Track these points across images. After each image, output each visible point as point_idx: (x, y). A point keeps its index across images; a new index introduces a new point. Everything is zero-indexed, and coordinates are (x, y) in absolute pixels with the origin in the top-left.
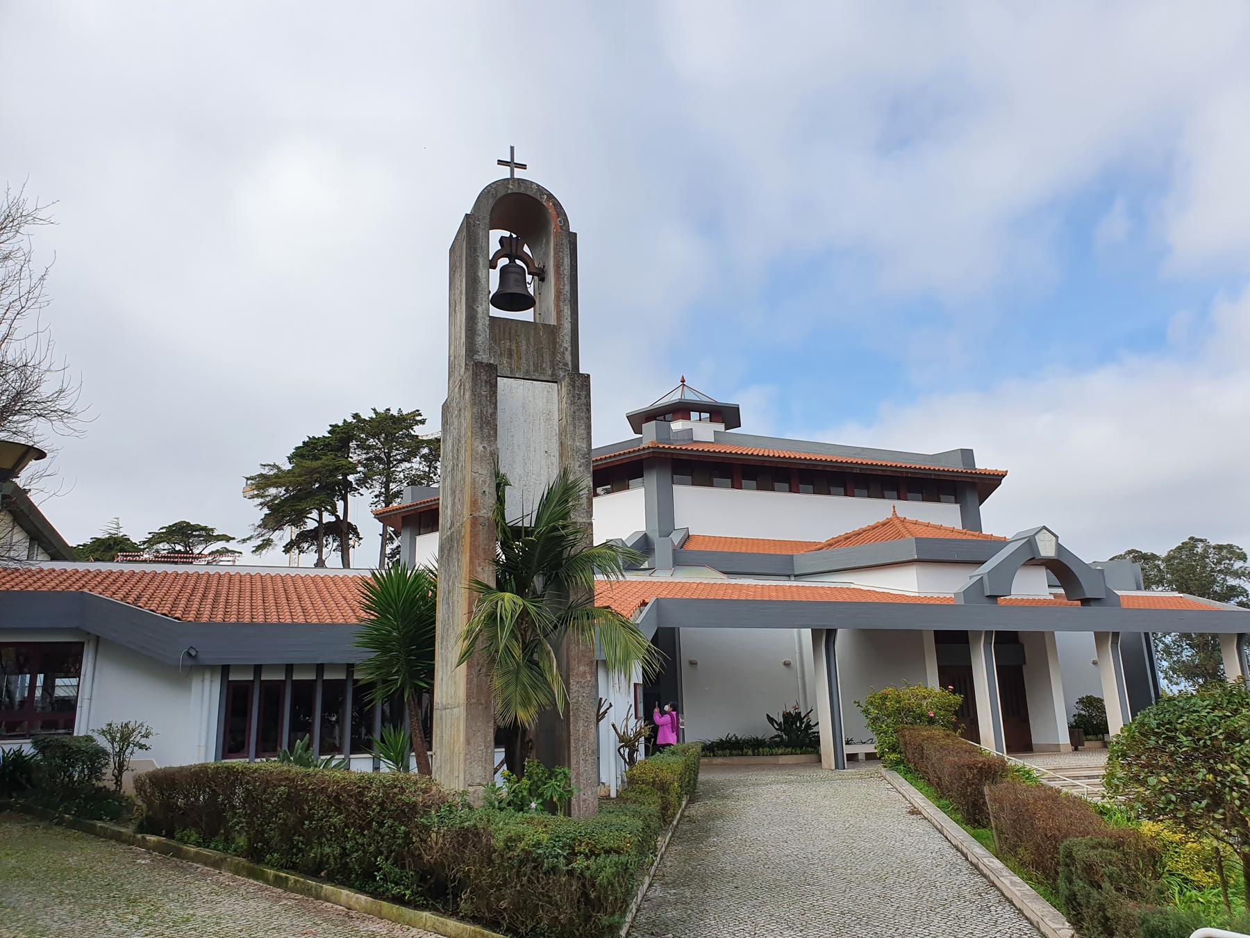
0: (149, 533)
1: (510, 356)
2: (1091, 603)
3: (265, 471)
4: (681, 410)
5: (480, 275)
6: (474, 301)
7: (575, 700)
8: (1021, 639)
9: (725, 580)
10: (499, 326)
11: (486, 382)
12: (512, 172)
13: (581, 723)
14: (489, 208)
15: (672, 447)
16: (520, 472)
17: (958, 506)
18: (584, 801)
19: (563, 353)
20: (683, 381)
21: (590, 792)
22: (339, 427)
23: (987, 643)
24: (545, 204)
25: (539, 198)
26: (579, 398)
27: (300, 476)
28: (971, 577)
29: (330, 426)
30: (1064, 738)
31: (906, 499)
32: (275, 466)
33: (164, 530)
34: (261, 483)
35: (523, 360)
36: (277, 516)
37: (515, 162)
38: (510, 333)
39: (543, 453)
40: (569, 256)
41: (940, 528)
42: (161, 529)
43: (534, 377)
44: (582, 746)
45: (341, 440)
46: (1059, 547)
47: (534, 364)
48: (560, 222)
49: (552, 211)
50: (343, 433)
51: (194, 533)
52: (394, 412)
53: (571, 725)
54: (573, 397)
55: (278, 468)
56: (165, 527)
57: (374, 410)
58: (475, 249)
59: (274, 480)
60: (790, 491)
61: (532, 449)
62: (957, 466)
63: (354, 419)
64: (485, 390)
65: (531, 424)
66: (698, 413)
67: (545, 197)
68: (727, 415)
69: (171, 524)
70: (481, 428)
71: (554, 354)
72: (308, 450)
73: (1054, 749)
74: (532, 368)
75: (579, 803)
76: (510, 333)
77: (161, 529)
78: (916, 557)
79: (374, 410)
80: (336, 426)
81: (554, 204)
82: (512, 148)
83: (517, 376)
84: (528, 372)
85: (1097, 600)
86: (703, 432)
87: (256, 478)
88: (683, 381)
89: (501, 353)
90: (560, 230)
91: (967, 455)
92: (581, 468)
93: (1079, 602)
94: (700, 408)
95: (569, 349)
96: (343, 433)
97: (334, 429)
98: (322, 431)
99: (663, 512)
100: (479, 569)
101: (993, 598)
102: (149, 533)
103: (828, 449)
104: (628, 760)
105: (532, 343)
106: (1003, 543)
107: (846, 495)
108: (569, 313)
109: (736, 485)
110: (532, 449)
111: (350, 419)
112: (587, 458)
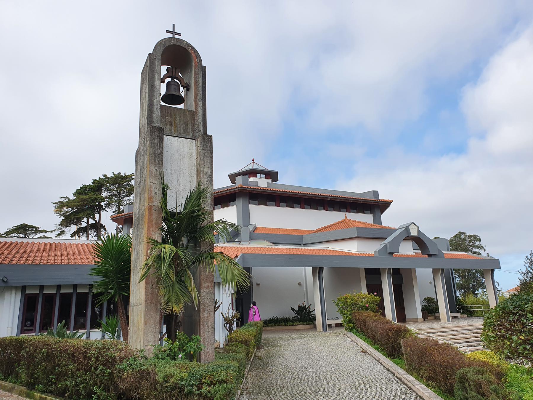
0: (8, 229)
1: (171, 124)
2: (432, 256)
3: (62, 200)
4: (252, 173)
5: (156, 83)
6: (152, 96)
7: (203, 301)
8: (401, 271)
9: (273, 246)
10: (165, 110)
11: (158, 136)
12: (174, 36)
13: (206, 312)
14: (161, 51)
15: (249, 187)
16: (175, 184)
17: (372, 215)
18: (208, 352)
19: (198, 125)
20: (253, 160)
21: (210, 348)
22: (96, 180)
23: (389, 274)
24: (190, 51)
25: (187, 48)
26: (207, 147)
27: (78, 202)
28: (381, 245)
29: (93, 180)
30: (420, 315)
32: (67, 198)
33: (15, 228)
34: (60, 206)
35: (178, 127)
36: (67, 221)
37: (175, 32)
38: (171, 113)
39: (188, 175)
40: (202, 77)
41: (366, 224)
42: (13, 227)
43: (183, 136)
44: (207, 324)
45: (98, 186)
46: (419, 232)
47: (183, 129)
48: (198, 60)
49: (193, 55)
50: (99, 183)
51: (29, 229)
52: (122, 174)
53: (201, 313)
54: (204, 146)
55: (68, 199)
56: (15, 226)
57: (113, 173)
58: (153, 71)
59: (66, 204)
60: (301, 208)
61: (182, 173)
62: (371, 198)
63: (104, 177)
64: (157, 140)
65: (181, 160)
66: (260, 175)
67: (190, 48)
68: (272, 176)
69: (18, 225)
70: (155, 160)
71: (193, 125)
72: (83, 191)
73: (416, 321)
74: (182, 132)
75: (205, 353)
76: (171, 113)
77: (13, 227)
78: (357, 236)
79: (113, 173)
80: (96, 180)
81: (195, 52)
82: (174, 25)
83: (174, 135)
84: (180, 133)
85: (435, 255)
86: (262, 183)
87: (58, 203)
88: (253, 160)
89: (166, 123)
90: (197, 65)
91: (376, 193)
92: (208, 183)
93: (427, 256)
94: (261, 172)
95: (202, 123)
96: (99, 183)
97: (95, 181)
98: (89, 182)
99: (245, 216)
100: (153, 233)
101: (391, 254)
102: (8, 229)
103: (316, 190)
104: (228, 330)
105: (182, 119)
106: (394, 230)
107: (324, 210)
108: (202, 105)
109: (277, 205)
110: (182, 173)
111: (102, 177)
112: (210, 177)
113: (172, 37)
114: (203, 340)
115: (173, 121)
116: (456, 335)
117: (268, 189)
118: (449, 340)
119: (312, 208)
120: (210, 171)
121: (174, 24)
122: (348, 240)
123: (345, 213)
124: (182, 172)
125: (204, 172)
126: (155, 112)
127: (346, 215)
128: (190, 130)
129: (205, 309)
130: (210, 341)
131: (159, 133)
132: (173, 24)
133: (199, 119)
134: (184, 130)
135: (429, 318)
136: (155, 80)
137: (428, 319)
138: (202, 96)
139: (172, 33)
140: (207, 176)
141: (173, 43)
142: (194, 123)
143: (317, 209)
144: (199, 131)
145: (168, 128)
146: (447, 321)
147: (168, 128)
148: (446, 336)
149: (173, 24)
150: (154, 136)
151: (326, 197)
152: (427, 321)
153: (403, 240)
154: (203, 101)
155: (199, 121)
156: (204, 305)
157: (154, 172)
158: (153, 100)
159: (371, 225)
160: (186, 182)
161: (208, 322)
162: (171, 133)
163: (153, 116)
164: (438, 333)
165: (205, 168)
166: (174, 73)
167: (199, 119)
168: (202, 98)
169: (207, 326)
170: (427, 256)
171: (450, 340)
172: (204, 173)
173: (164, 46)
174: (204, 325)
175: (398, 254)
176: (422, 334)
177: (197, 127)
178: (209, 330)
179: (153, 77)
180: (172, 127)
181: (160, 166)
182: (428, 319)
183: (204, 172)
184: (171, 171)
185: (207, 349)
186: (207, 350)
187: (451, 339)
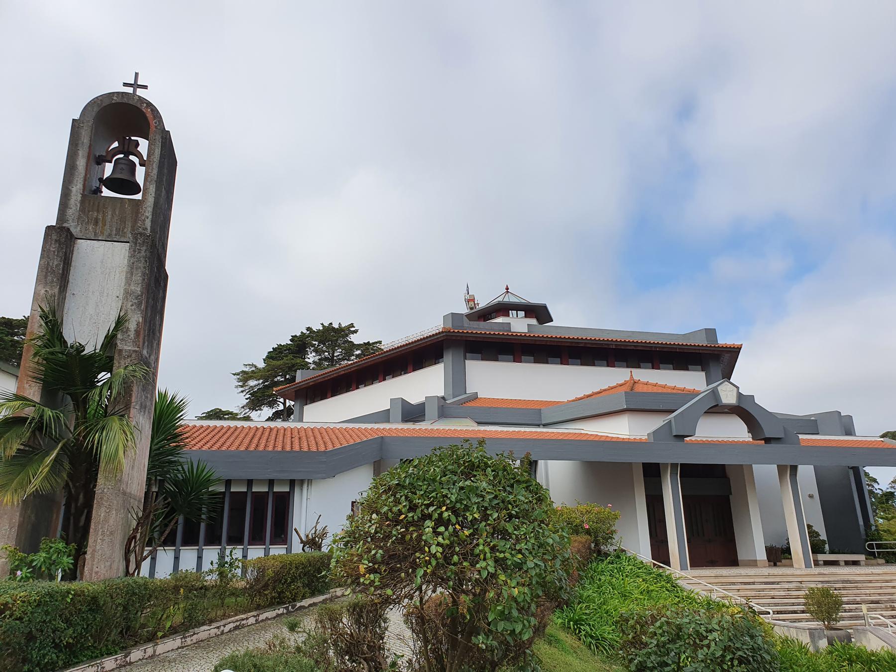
0: (196, 417)
1: (96, 222)
2: (772, 442)
3: (247, 369)
4: (502, 309)
5: (78, 163)
6: (70, 183)
7: (100, 491)
8: (729, 473)
9: (477, 428)
10: (90, 201)
11: (56, 241)
12: (135, 91)
13: (103, 509)
14: (94, 114)
15: (465, 331)
16: (91, 313)
17: (703, 374)
18: (97, 573)
19: (144, 220)
20: (507, 289)
21: (103, 566)
22: (297, 336)
23: (673, 474)
24: (144, 110)
25: (139, 106)
26: (139, 252)
27: (268, 371)
28: (664, 421)
29: (292, 336)
30: (761, 555)
31: (659, 369)
32: (253, 365)
33: (205, 415)
34: (244, 377)
35: (107, 226)
36: (257, 401)
37: (139, 84)
38: (98, 206)
39: (115, 298)
40: (160, 148)
41: (664, 387)
42: (203, 414)
43: (115, 239)
44: (102, 528)
45: (298, 346)
46: (740, 396)
47: (116, 229)
48: (156, 123)
49: (149, 115)
50: (299, 341)
51: (225, 417)
52: (336, 326)
53: (94, 511)
54: (134, 251)
55: (256, 367)
56: (205, 413)
57: (322, 324)
58: (77, 145)
59: (251, 374)
60: (561, 364)
61: (105, 294)
62: (702, 341)
63: (308, 331)
64: (54, 247)
65: (107, 275)
66: (516, 312)
67: (145, 105)
68: (539, 313)
69: (209, 411)
70: (46, 277)
71: (135, 221)
72: (277, 353)
73: (753, 564)
74: (114, 232)
75: (91, 574)
76: (98, 206)
77: (203, 414)
78: (625, 407)
79: (322, 324)
80: (296, 336)
81: (152, 110)
82: (137, 74)
83: (100, 239)
84: (110, 235)
85: (777, 440)
86: (519, 324)
87: (239, 374)
88: (507, 289)
89: (88, 221)
90: (155, 129)
91: (711, 333)
92: (133, 307)
93: (764, 441)
94: (517, 307)
95: (150, 217)
96: (299, 341)
97: (294, 339)
98: (286, 341)
99: (457, 380)
100: (27, 386)
101: (681, 437)
102: (196, 417)
103: (608, 334)
104: (134, 540)
105: (117, 213)
106: (698, 393)
107: (608, 366)
108: (154, 190)
109: (517, 360)
110: (105, 294)
111: (305, 331)
112: (139, 299)
113: (132, 92)
114: (91, 552)
115: (100, 217)
116: (794, 590)
117: (494, 333)
118: (770, 597)
119: (583, 364)
120: (139, 289)
121: (137, 72)
122: (618, 415)
123: (629, 370)
124: (105, 293)
125: (130, 291)
126: (72, 206)
127: (631, 372)
128: (128, 230)
129: (102, 504)
130: (104, 556)
131: (59, 235)
132: (136, 73)
133: (147, 212)
134: (118, 230)
135: (783, 561)
136: (78, 158)
137: (781, 562)
138: (157, 177)
139: (132, 87)
140: (134, 298)
141: (115, 100)
142: (137, 217)
143: (547, 363)
144: (144, 230)
145: (90, 228)
146: (804, 566)
147: (90, 228)
148: (768, 590)
149: (136, 73)
150: (50, 240)
151: (606, 343)
152: (779, 566)
153: (705, 413)
154: (156, 184)
155: (147, 214)
156: (100, 498)
157: (41, 294)
158: (70, 188)
159: (674, 389)
160: (111, 309)
161: (105, 524)
162: (95, 235)
163: (68, 211)
164: (754, 584)
165: (132, 285)
166: (126, 147)
167: (147, 212)
168: (155, 179)
169: (102, 532)
170: (764, 441)
171: (773, 598)
172: (128, 292)
173: (100, 106)
174: (96, 529)
175: (693, 438)
176: (686, 578)
177: (141, 224)
178: (104, 538)
179: (75, 154)
180: (98, 227)
181: (54, 286)
182: (781, 562)
183: (130, 291)
184: (86, 294)
185: (97, 568)
186: (97, 569)
187: (776, 597)
